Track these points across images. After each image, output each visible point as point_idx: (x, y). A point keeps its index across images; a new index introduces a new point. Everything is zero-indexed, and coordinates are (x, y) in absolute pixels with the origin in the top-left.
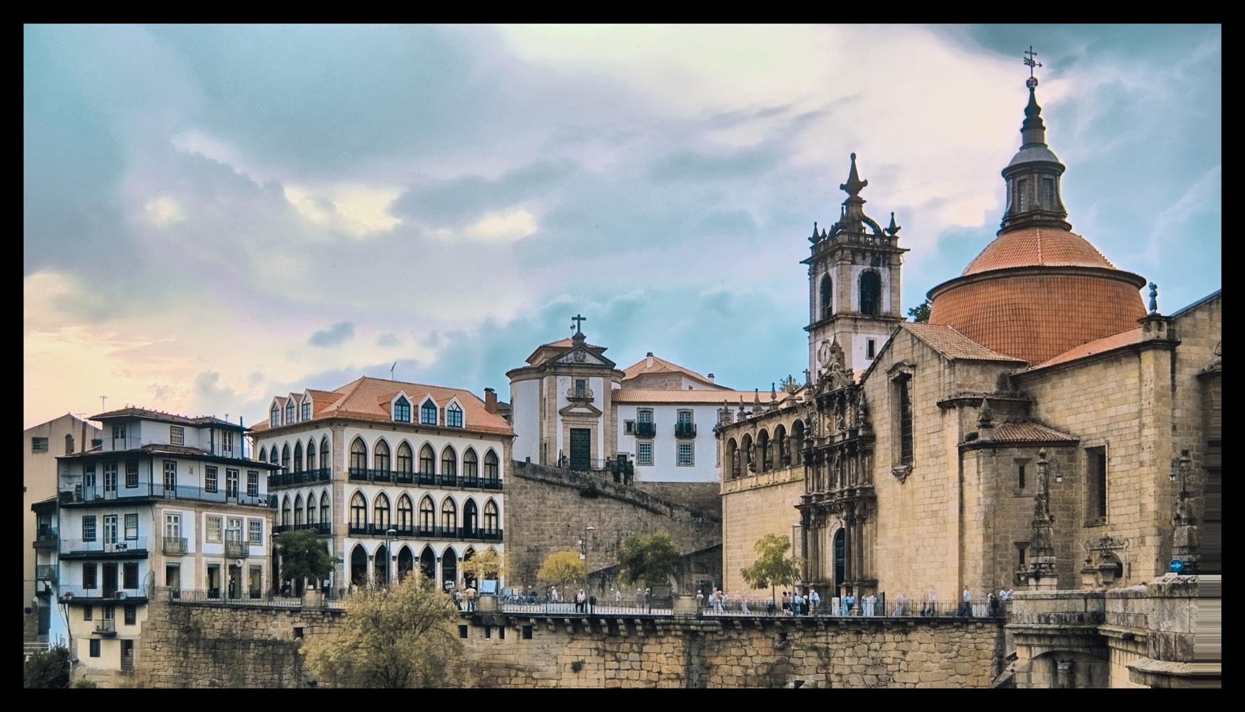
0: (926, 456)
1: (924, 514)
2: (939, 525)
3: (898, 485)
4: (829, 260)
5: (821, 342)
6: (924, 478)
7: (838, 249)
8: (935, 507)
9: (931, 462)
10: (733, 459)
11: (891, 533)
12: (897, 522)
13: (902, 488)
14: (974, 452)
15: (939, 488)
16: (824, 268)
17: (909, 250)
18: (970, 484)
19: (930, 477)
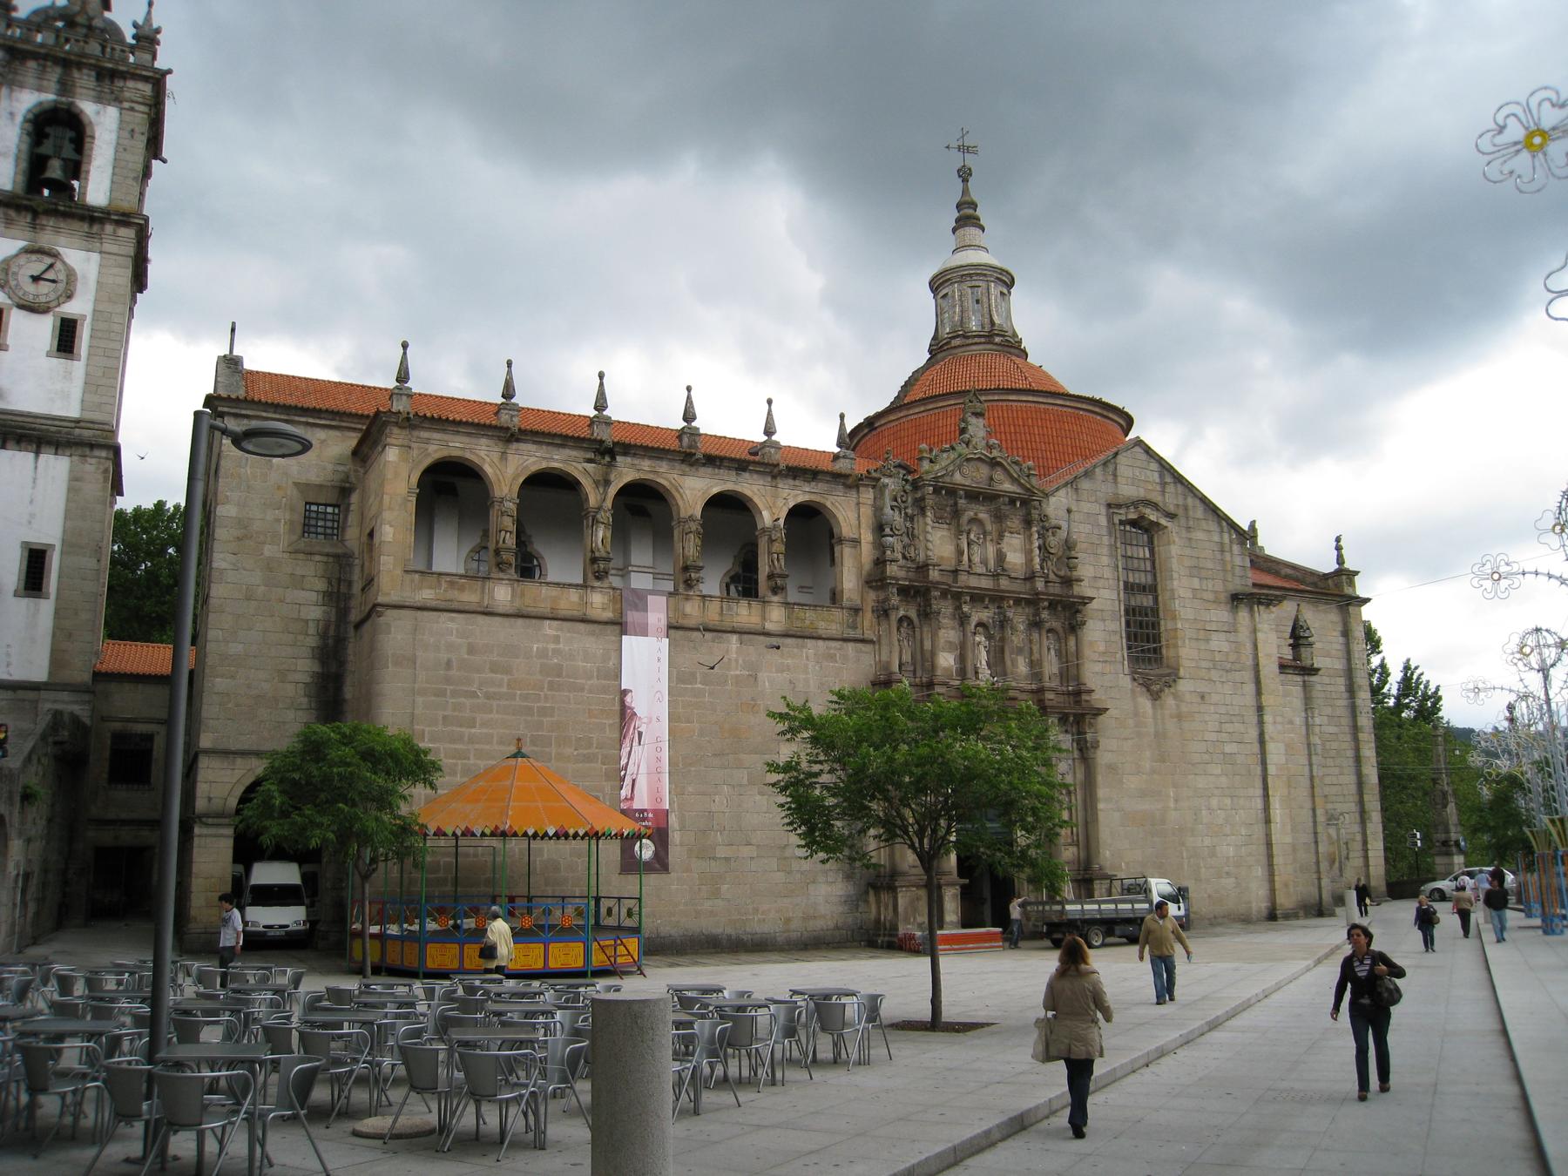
0: (1204, 664)
1: (1206, 757)
2: (1238, 777)
3: (1145, 703)
4: (84, 80)
5: (22, 244)
6: (1203, 697)
7: (146, 79)
8: (1229, 748)
9: (1214, 675)
10: (330, 505)
11: (1133, 782)
12: (1147, 765)
13: (1154, 707)
14: (1299, 678)
15: (1234, 719)
16: (53, 85)
17: (164, 161)
18: (1291, 722)
19: (1215, 698)
